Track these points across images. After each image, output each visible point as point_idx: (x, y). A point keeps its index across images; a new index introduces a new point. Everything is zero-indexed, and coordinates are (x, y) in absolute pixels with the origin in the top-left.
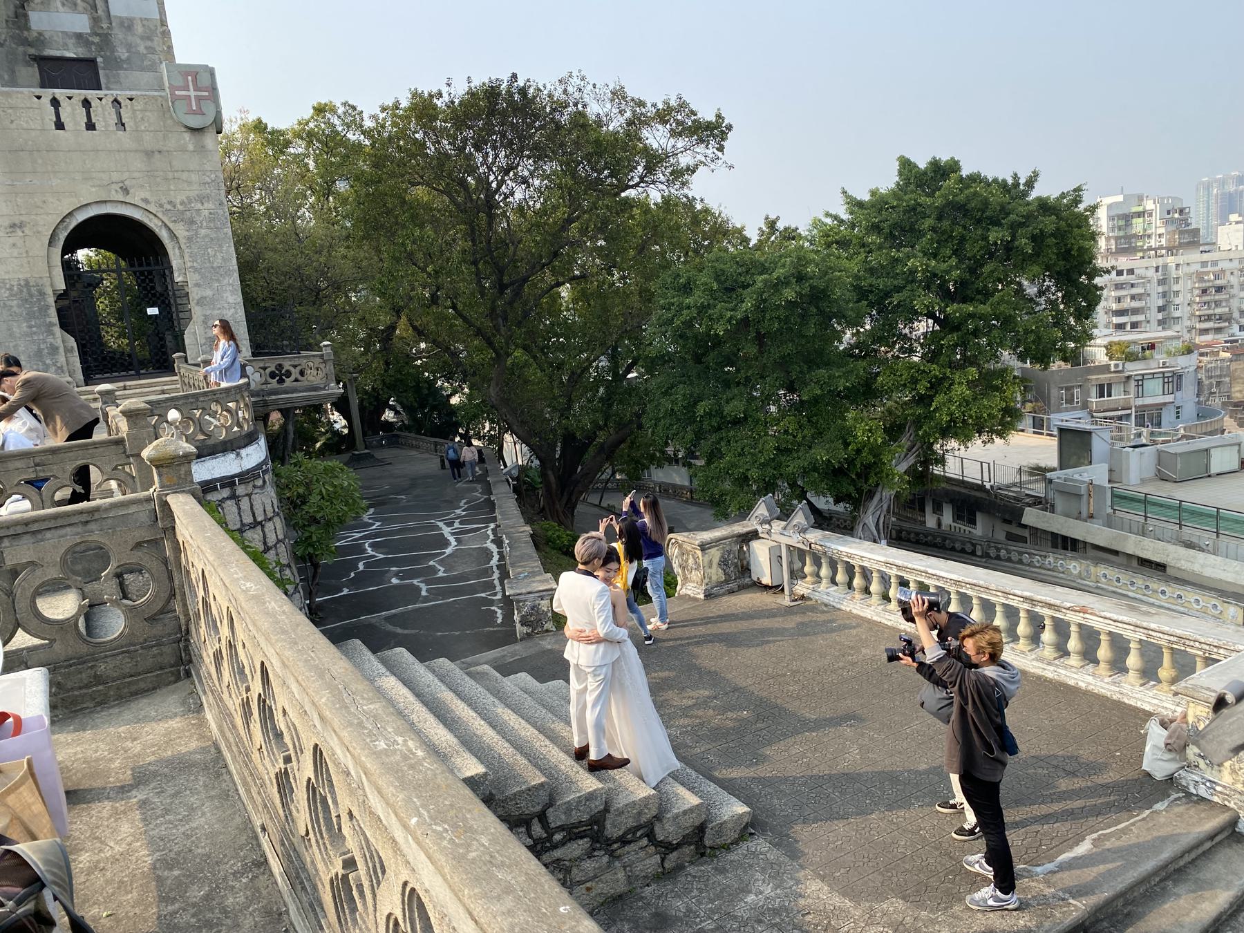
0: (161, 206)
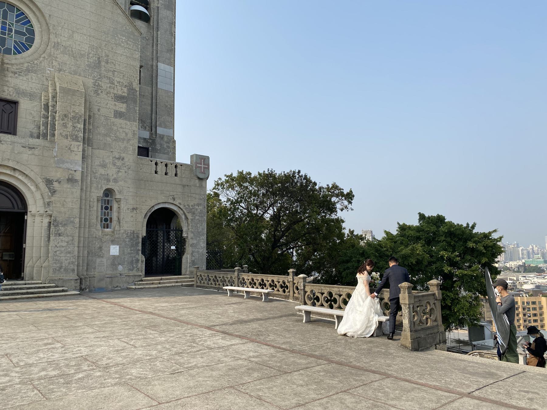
0: (185, 206)
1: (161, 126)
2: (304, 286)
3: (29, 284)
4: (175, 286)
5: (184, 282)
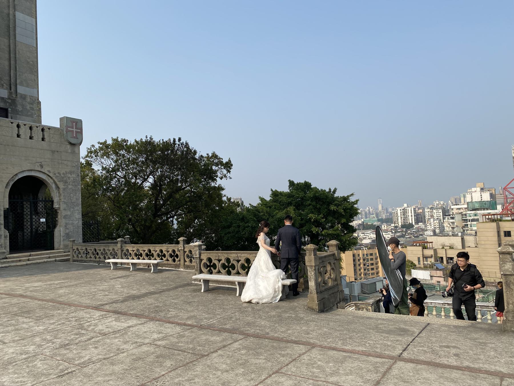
0: (55, 174)
1: (21, 84)
2: (200, 254)
4: (47, 262)
5: (58, 256)
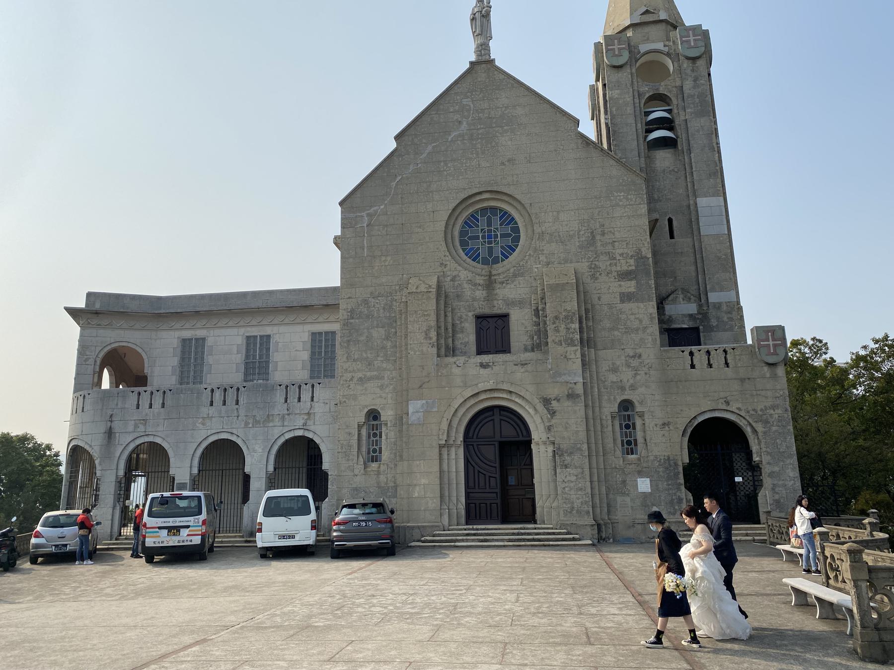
0: (748, 412)
1: (713, 290)
3: (539, 529)
